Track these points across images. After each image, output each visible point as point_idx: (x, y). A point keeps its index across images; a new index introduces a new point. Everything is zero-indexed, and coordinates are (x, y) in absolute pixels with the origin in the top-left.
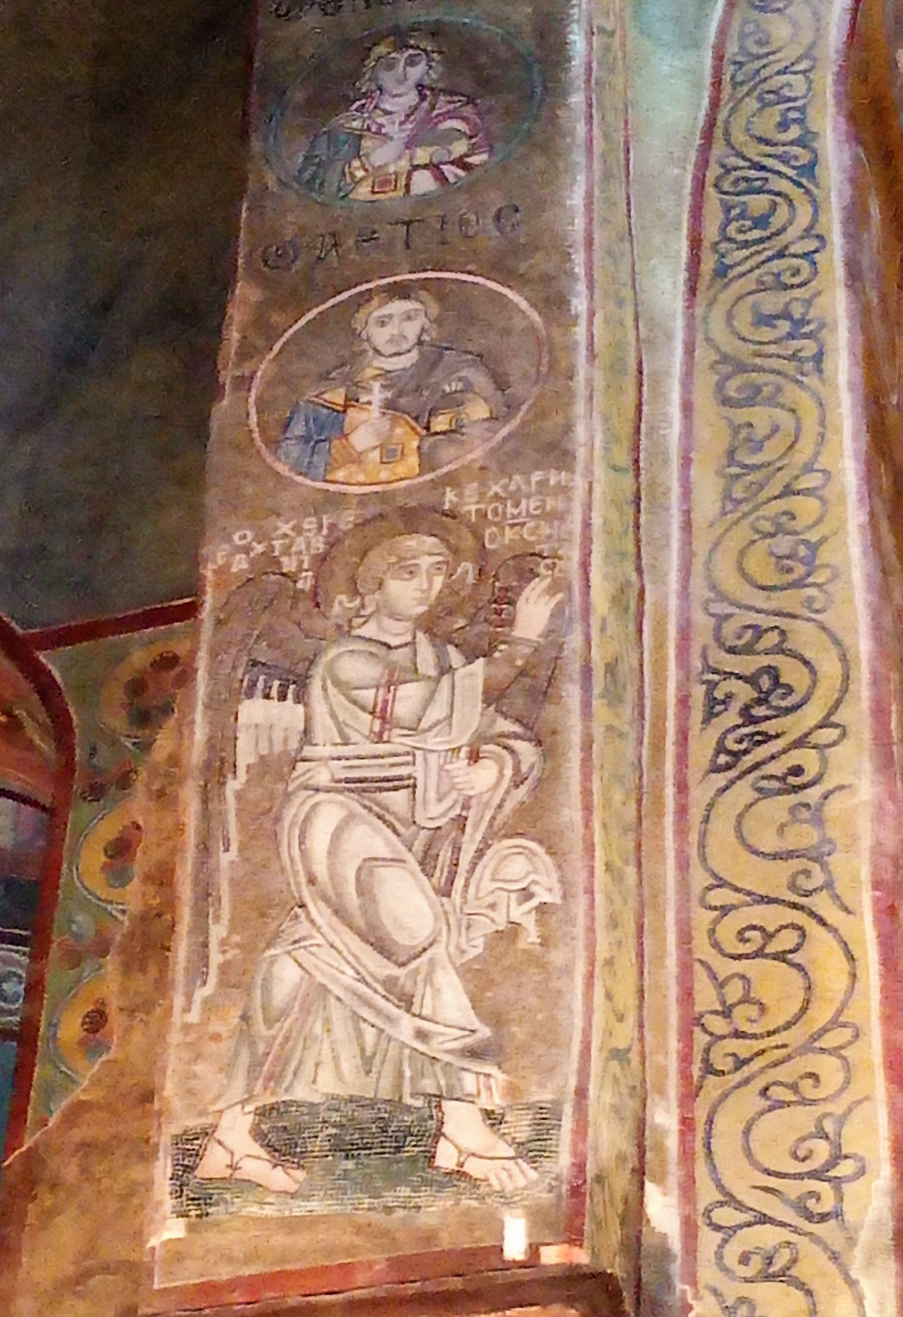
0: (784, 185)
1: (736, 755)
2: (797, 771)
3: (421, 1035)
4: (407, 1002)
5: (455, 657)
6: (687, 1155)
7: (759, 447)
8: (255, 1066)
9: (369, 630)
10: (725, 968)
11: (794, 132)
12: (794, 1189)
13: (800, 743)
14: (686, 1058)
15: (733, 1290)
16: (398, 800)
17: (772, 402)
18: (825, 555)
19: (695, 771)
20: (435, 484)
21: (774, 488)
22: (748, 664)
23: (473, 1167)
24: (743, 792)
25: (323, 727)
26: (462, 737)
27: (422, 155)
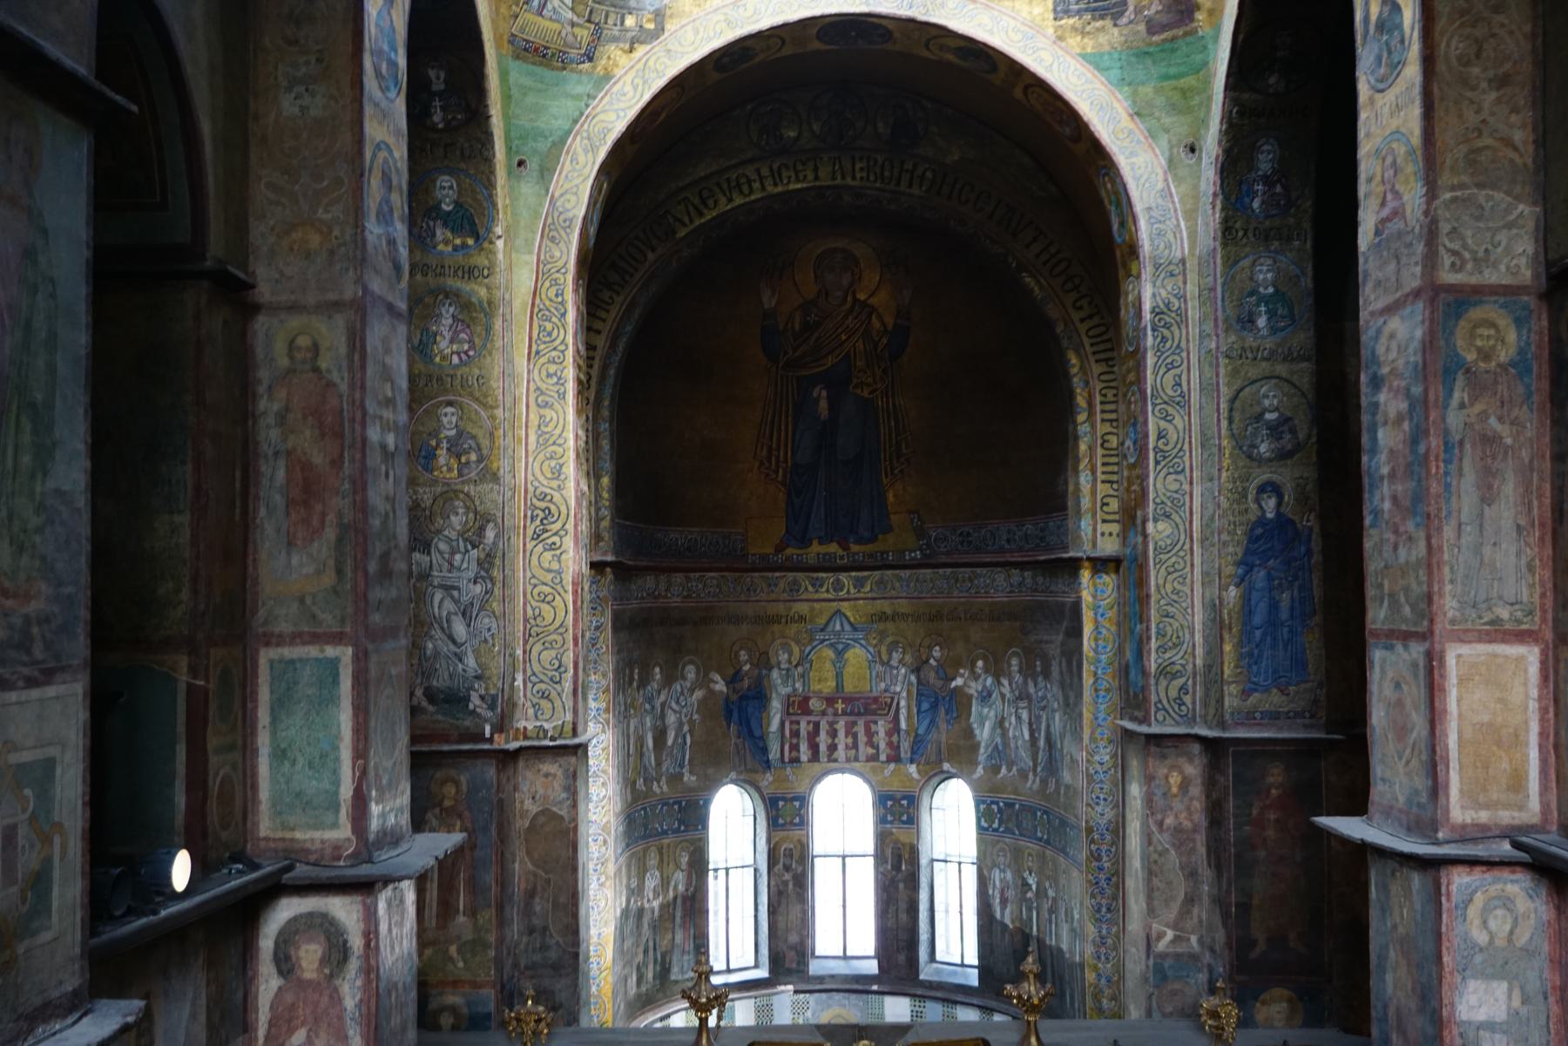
0: (554, 319)
1: (539, 536)
2: (554, 544)
3: (464, 670)
4: (460, 660)
5: (469, 547)
6: (525, 662)
7: (547, 426)
8: (423, 673)
9: (446, 533)
10: (534, 603)
11: (560, 299)
12: (550, 674)
13: (556, 534)
14: (524, 634)
15: (535, 700)
16: (455, 593)
17: (551, 407)
18: (564, 470)
19: (528, 540)
20: (463, 482)
21: (551, 442)
22: (543, 505)
23: (478, 710)
24: (540, 548)
25: (434, 562)
26: (471, 575)
27: (455, 347)
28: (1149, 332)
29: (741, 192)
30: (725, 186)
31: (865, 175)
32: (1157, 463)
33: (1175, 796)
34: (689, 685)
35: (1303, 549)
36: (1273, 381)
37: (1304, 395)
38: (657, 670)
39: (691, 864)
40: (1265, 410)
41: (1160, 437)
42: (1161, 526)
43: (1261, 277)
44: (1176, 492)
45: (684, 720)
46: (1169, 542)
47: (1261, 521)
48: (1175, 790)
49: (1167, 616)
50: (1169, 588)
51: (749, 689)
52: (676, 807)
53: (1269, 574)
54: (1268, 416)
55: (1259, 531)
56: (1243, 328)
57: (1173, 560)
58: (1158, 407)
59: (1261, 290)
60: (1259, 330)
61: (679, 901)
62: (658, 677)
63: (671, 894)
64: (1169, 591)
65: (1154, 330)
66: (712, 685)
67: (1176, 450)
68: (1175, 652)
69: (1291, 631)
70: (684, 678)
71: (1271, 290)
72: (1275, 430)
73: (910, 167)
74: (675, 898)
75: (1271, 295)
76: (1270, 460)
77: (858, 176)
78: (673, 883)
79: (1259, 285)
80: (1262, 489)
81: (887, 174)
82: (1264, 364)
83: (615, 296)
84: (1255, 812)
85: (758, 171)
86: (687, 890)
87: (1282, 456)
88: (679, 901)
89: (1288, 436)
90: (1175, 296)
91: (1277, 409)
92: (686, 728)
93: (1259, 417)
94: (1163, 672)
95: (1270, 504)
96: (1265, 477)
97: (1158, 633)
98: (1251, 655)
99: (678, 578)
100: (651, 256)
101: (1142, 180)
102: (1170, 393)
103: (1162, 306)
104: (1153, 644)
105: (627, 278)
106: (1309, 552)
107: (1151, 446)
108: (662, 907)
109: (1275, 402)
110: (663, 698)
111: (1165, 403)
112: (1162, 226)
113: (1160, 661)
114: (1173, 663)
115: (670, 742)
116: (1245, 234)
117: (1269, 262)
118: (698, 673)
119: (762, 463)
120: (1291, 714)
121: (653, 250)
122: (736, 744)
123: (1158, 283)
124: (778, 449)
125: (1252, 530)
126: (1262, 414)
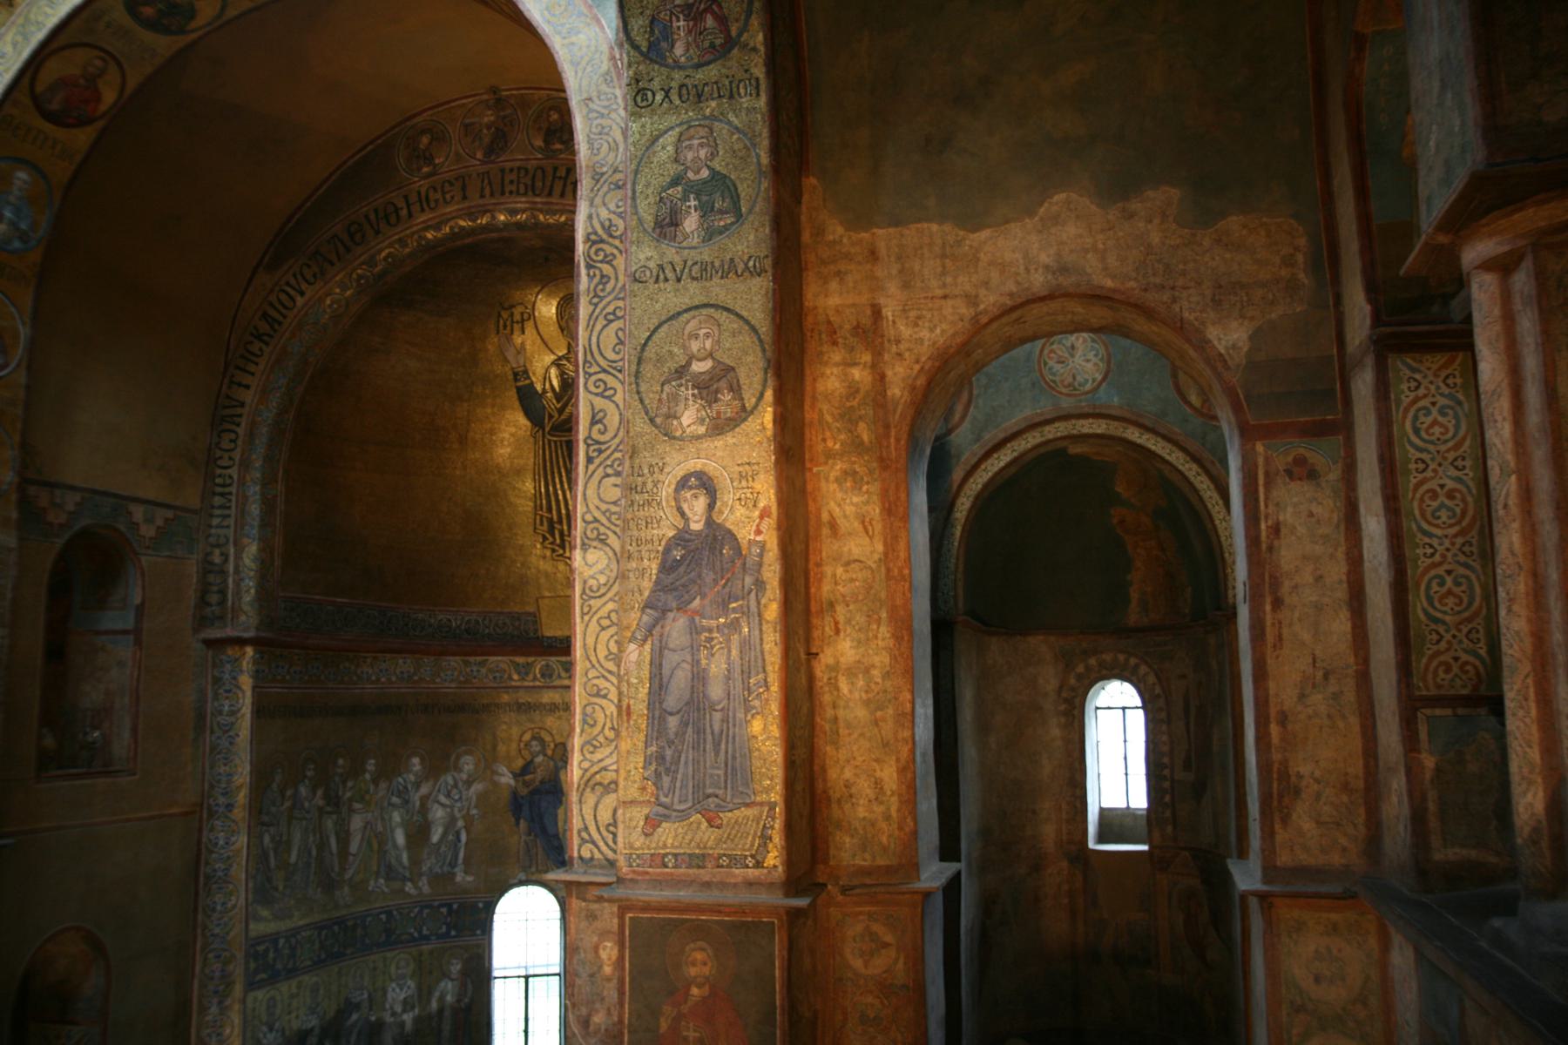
28: (583, 271)
29: (388, 223)
30: (372, 217)
31: (514, 188)
32: (589, 460)
33: (609, 980)
34: (464, 776)
35: (748, 580)
36: (705, 311)
37: (753, 329)
38: (416, 760)
39: (465, 973)
40: (691, 358)
41: (594, 422)
42: (592, 556)
43: (690, 156)
44: (614, 503)
45: (458, 815)
46: (603, 580)
47: (683, 538)
48: (607, 970)
49: (598, 695)
50: (602, 653)
51: (542, 782)
52: (444, 910)
53: (693, 621)
54: (698, 367)
55: (677, 554)
56: (663, 235)
57: (611, 606)
58: (594, 378)
59: (690, 175)
60: (686, 237)
61: (447, 1013)
62: (417, 768)
63: (434, 1005)
64: (601, 655)
65: (589, 267)
66: (496, 778)
67: (617, 441)
68: (608, 750)
69: (725, 720)
70: (460, 771)
71: (705, 173)
72: (706, 389)
73: (563, 174)
74: (441, 1011)
75: (705, 182)
76: (698, 437)
77: (507, 189)
78: (437, 994)
79: (687, 168)
80: (683, 484)
81: (539, 184)
82: (693, 287)
83: (264, 347)
84: (664, 1025)
85: (406, 197)
86: (459, 1001)
87: (719, 427)
88: (447, 1013)
89: (727, 397)
90: (620, 215)
91: (711, 355)
92: (460, 823)
93: (681, 371)
94: (589, 783)
95: (697, 507)
96: (695, 464)
97: (584, 722)
98: (660, 758)
99: (454, 661)
100: (300, 301)
101: (584, 63)
102: (612, 356)
103: (600, 231)
104: (577, 741)
105: (276, 326)
106: (760, 585)
107: (581, 436)
108: (417, 1020)
109: (708, 344)
110: (424, 790)
111: (604, 371)
112: (604, 122)
113: (586, 765)
114: (605, 769)
115: (435, 838)
116: (667, 96)
117: (703, 132)
118: (476, 765)
119: (545, 538)
120: (724, 861)
121: (302, 294)
122: (525, 842)
123: (598, 200)
124: (560, 522)
125: (667, 550)
126: (689, 364)
